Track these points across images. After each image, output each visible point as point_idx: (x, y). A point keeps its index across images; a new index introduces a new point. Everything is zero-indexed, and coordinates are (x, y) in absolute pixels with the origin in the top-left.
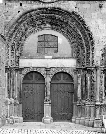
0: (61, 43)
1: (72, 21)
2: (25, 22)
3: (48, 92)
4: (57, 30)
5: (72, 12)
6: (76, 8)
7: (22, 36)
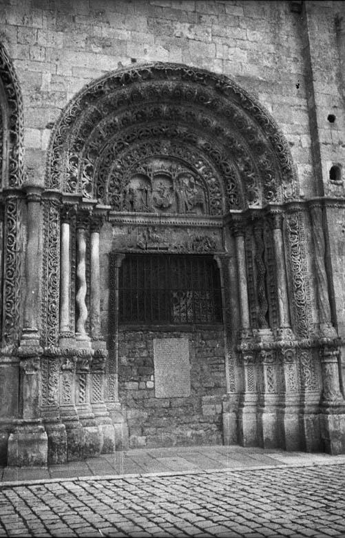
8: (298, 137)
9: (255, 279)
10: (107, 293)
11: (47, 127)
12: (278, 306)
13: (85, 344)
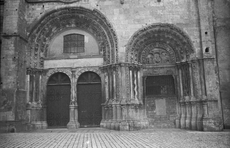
0: (87, 42)
1: (96, 19)
2: (48, 23)
3: (74, 93)
4: (83, 29)
5: (94, 10)
6: (97, 5)
7: (47, 37)
8: (196, 40)
9: (184, 82)
10: (142, 87)
11: (125, 46)
12: (190, 90)
13: (137, 102)
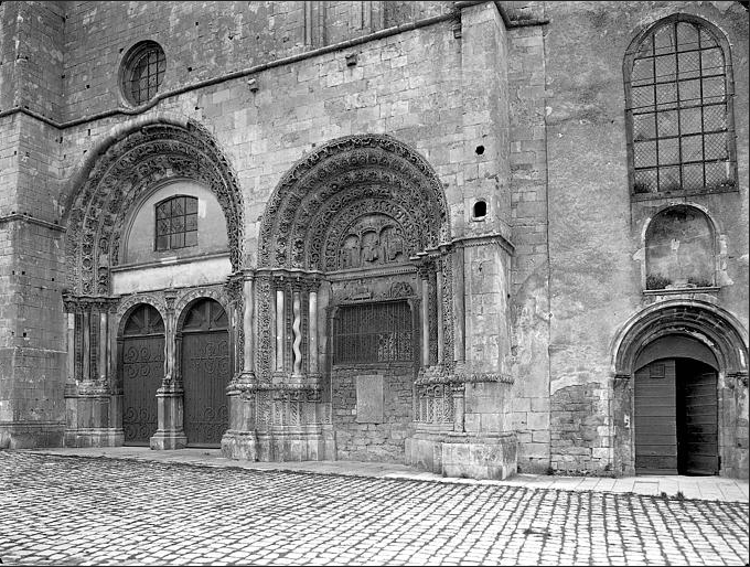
0: (204, 216)
4: (190, 179)
8: (454, 176)
